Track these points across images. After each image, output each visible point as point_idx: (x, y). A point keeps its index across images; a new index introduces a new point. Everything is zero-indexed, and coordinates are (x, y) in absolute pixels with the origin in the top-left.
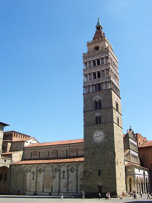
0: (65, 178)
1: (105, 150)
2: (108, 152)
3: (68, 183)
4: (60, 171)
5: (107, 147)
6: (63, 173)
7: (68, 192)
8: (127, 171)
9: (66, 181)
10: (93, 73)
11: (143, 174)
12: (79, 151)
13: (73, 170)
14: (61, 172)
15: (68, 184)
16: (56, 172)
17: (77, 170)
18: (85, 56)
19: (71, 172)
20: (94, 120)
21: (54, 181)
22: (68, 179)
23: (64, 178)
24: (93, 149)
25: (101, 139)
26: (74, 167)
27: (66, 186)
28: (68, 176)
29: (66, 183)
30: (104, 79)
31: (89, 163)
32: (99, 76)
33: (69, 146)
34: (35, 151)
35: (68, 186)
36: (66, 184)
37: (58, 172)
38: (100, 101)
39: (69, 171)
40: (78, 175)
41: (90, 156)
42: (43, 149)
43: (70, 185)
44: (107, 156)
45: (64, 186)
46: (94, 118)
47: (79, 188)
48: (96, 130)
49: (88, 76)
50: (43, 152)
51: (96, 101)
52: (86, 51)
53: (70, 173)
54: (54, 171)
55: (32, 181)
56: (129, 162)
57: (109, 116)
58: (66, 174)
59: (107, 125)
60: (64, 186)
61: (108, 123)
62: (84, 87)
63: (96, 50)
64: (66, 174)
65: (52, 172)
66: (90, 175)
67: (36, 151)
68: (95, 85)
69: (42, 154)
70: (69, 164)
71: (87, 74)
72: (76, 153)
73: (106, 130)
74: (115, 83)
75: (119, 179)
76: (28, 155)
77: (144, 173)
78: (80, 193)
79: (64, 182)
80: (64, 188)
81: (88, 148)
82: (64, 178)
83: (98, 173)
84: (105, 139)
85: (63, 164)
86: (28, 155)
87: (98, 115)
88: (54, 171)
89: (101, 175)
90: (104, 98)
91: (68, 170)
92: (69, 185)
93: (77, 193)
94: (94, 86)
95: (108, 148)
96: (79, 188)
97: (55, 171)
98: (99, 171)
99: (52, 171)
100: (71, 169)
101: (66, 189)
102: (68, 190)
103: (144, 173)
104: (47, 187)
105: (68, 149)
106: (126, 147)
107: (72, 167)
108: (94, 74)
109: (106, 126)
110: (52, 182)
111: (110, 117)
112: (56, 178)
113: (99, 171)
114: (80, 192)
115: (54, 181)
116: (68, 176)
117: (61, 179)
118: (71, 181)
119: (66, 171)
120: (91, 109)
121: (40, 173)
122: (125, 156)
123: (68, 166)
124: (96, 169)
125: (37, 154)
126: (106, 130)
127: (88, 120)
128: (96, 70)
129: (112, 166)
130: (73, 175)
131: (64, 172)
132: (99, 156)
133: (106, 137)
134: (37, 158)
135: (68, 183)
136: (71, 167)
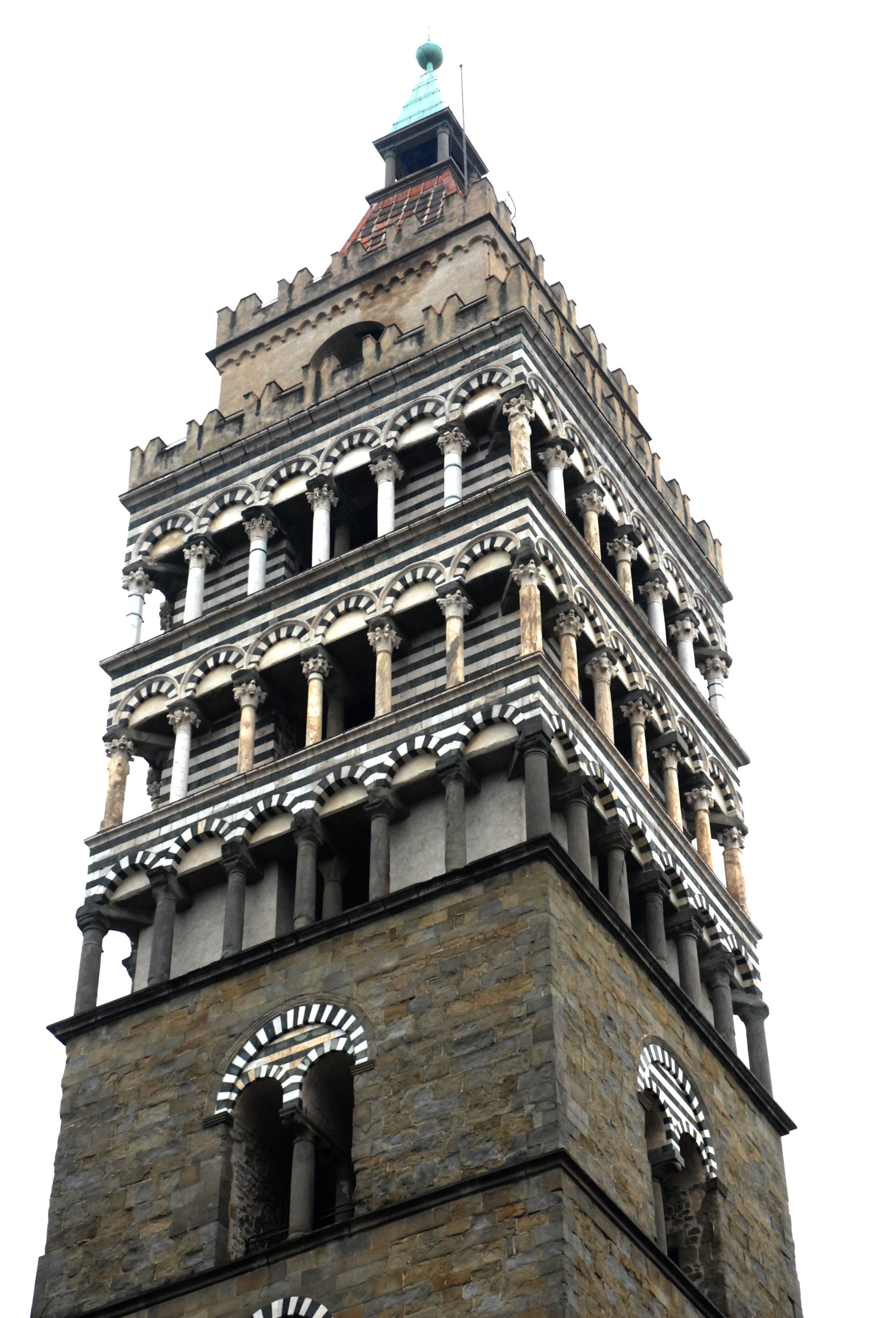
18: (153, 491)
30: (428, 734)
32: (352, 705)
38: (333, 1075)
49: (183, 740)
51: (266, 1091)
52: (185, 396)
62: (95, 919)
68: (280, 855)
71: (161, 727)
74: (632, 809)
94: (253, 880)
108: (281, 690)
128: (312, 630)
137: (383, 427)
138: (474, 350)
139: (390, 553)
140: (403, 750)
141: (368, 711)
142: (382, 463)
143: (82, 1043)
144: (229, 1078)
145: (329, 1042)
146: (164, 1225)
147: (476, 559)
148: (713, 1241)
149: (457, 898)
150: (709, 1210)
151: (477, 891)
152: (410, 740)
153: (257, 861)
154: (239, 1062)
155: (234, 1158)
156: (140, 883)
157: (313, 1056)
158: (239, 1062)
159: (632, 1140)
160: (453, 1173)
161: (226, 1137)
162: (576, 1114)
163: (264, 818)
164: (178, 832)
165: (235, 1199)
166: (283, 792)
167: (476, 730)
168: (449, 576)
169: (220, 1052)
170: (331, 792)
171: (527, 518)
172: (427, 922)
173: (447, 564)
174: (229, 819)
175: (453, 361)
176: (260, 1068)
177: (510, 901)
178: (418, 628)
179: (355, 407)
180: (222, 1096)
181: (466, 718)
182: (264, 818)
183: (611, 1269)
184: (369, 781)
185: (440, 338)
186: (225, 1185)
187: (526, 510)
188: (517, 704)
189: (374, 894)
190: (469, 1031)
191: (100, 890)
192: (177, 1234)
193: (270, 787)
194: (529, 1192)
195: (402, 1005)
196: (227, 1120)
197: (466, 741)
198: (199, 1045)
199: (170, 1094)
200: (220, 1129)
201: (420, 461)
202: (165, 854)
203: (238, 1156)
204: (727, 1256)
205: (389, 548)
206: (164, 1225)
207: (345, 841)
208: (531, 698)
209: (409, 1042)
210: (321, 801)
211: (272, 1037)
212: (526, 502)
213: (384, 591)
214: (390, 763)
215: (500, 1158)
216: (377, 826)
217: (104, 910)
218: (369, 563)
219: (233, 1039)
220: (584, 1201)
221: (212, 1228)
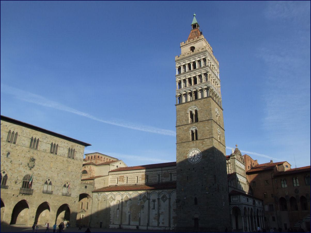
0: (156, 209)
3: (159, 215)
4: (149, 199)
6: (153, 202)
7: (158, 225)
8: (232, 200)
9: (156, 212)
10: (189, 78)
11: (252, 205)
12: (174, 176)
13: (165, 199)
14: (151, 201)
15: (159, 216)
16: (145, 201)
17: (170, 199)
19: (162, 201)
21: (142, 211)
22: (159, 209)
23: (154, 209)
26: (166, 195)
27: (157, 218)
28: (159, 205)
29: (156, 214)
33: (162, 170)
34: (121, 177)
35: (159, 218)
36: (157, 215)
37: (147, 201)
39: (161, 200)
40: (171, 205)
42: (132, 174)
43: (161, 217)
45: (154, 218)
47: (172, 221)
48: (191, 148)
53: (162, 202)
54: (142, 200)
56: (235, 188)
58: (156, 203)
59: (204, 141)
60: (155, 219)
61: (206, 140)
63: (192, 51)
64: (156, 203)
65: (140, 201)
67: (123, 176)
69: (130, 179)
70: (160, 191)
72: (169, 178)
76: (113, 181)
77: (254, 203)
78: (173, 227)
79: (154, 213)
80: (153, 220)
81: (181, 170)
82: (154, 209)
85: (153, 191)
86: (113, 181)
87: (194, 130)
88: (142, 200)
91: (159, 199)
92: (160, 217)
93: (170, 226)
96: (172, 221)
100: (163, 197)
101: (157, 222)
102: (159, 223)
103: (254, 203)
105: (160, 174)
107: (164, 195)
109: (204, 143)
114: (174, 226)
116: (159, 205)
117: (151, 209)
118: (162, 212)
119: (157, 201)
122: (228, 181)
123: (159, 194)
127: (181, 136)
130: (164, 205)
131: (154, 201)
134: (124, 184)
135: (159, 215)
136: (162, 195)
138: (203, 53)
139: (197, 70)
152: (200, 86)
160: (205, 120)
166: (191, 89)
169: (187, 108)
171: (208, 69)
175: (201, 53)
179: (193, 56)
185: (200, 51)
189: (198, 98)
194: (210, 121)
199: (184, 111)
205: (197, 69)
208: (209, 84)
212: (208, 67)
215: (208, 119)
218: (196, 70)
219: (188, 107)
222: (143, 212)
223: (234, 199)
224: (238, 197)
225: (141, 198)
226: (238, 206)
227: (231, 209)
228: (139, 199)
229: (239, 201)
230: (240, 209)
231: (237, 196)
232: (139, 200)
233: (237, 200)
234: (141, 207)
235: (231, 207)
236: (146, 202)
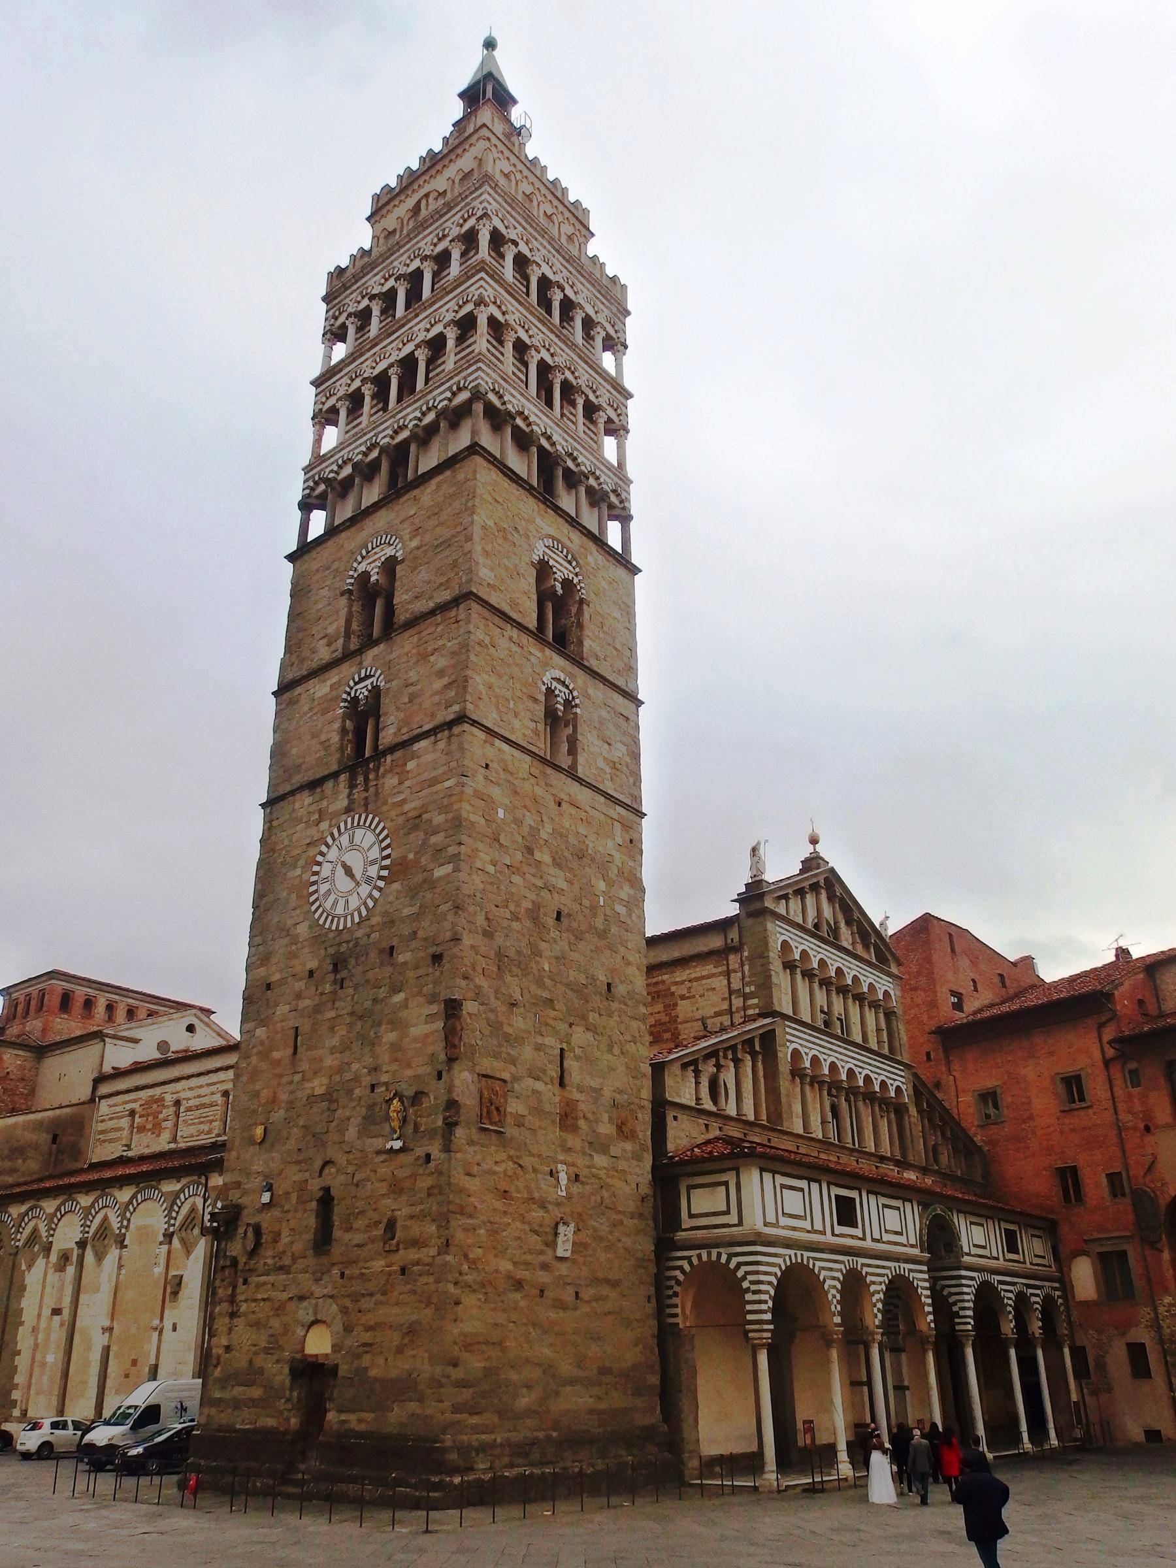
1: (382, 992)
2: (405, 1004)
5: (401, 958)
11: (916, 1251)
20: (335, 738)
24: (299, 996)
25: (365, 890)
31: (259, 1131)
32: (407, 387)
38: (390, 566)
41: (278, 1063)
44: (395, 1047)
46: (337, 725)
50: (197, 1102)
55: (48, 1329)
57: (441, 673)
62: (306, 506)
65: (165, 1248)
66: (258, 1244)
68: (374, 467)
73: (406, 808)
75: (519, 1285)
83: (312, 1221)
84: (396, 886)
89: (336, 1251)
90: (415, 543)
95: (405, 963)
97: (183, 1241)
98: (326, 1201)
99: (169, 1237)
104: (127, 1376)
106: (737, 1002)
110: (156, 1335)
111: (445, 681)
112: (184, 1293)
113: (326, 1201)
115: (168, 1325)
120: (324, 653)
121: (100, 1257)
124: (302, 1186)
125: (161, 1116)
126: (404, 801)
129: (420, 1151)
132: (333, 1050)
133: (397, 870)
137: (426, 244)
140: (424, 408)
141: (413, 390)
142: (425, 264)
143: (298, 563)
144: (351, 573)
145: (389, 551)
146: (324, 641)
147: (460, 307)
148: (580, 626)
149: (441, 477)
150: (580, 611)
151: (448, 473)
153: (366, 472)
154: (355, 565)
155: (354, 609)
156: (322, 487)
157: (383, 559)
158: (355, 565)
159: (528, 582)
161: (350, 599)
162: (485, 573)
163: (370, 449)
164: (337, 461)
165: (355, 626)
167: (454, 394)
168: (449, 316)
170: (396, 432)
172: (428, 491)
173: (449, 309)
174: (356, 451)
176: (361, 568)
177: (461, 476)
178: (437, 345)
180: (348, 581)
181: (450, 388)
182: (370, 449)
183: (503, 643)
184: (410, 426)
186: (348, 622)
187: (482, 278)
188: (470, 379)
190: (441, 540)
191: (307, 491)
192: (329, 645)
193: (372, 434)
195: (416, 531)
196: (350, 592)
197: (450, 400)
198: (340, 559)
200: (346, 596)
201: (443, 260)
202: (332, 471)
203: (356, 607)
204: (586, 632)
206: (324, 641)
207: (399, 455)
209: (418, 548)
210: (392, 438)
211: (368, 552)
213: (421, 330)
214: (419, 415)
216: (413, 448)
217: (309, 501)
220: (487, 614)
221: (341, 641)
222: (174, 1329)
223: (703, 1202)
224: (726, 1184)
225: (171, 1229)
226: (724, 1259)
227: (678, 1283)
228: (161, 1238)
229: (733, 1218)
230: (744, 1278)
231: (723, 1178)
232: (161, 1243)
233: (725, 1209)
234: (169, 1290)
235: (681, 1269)
236: (192, 1256)
